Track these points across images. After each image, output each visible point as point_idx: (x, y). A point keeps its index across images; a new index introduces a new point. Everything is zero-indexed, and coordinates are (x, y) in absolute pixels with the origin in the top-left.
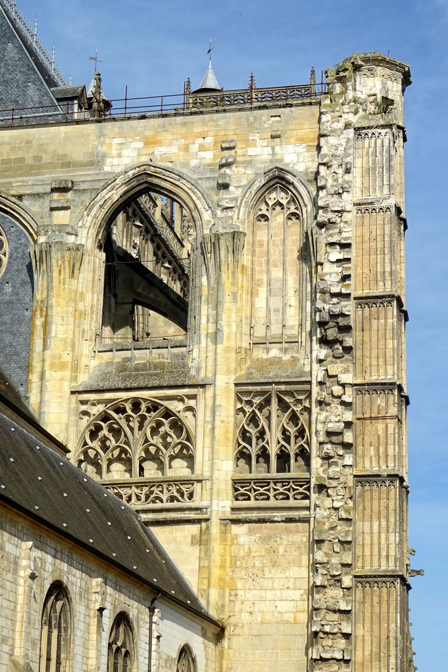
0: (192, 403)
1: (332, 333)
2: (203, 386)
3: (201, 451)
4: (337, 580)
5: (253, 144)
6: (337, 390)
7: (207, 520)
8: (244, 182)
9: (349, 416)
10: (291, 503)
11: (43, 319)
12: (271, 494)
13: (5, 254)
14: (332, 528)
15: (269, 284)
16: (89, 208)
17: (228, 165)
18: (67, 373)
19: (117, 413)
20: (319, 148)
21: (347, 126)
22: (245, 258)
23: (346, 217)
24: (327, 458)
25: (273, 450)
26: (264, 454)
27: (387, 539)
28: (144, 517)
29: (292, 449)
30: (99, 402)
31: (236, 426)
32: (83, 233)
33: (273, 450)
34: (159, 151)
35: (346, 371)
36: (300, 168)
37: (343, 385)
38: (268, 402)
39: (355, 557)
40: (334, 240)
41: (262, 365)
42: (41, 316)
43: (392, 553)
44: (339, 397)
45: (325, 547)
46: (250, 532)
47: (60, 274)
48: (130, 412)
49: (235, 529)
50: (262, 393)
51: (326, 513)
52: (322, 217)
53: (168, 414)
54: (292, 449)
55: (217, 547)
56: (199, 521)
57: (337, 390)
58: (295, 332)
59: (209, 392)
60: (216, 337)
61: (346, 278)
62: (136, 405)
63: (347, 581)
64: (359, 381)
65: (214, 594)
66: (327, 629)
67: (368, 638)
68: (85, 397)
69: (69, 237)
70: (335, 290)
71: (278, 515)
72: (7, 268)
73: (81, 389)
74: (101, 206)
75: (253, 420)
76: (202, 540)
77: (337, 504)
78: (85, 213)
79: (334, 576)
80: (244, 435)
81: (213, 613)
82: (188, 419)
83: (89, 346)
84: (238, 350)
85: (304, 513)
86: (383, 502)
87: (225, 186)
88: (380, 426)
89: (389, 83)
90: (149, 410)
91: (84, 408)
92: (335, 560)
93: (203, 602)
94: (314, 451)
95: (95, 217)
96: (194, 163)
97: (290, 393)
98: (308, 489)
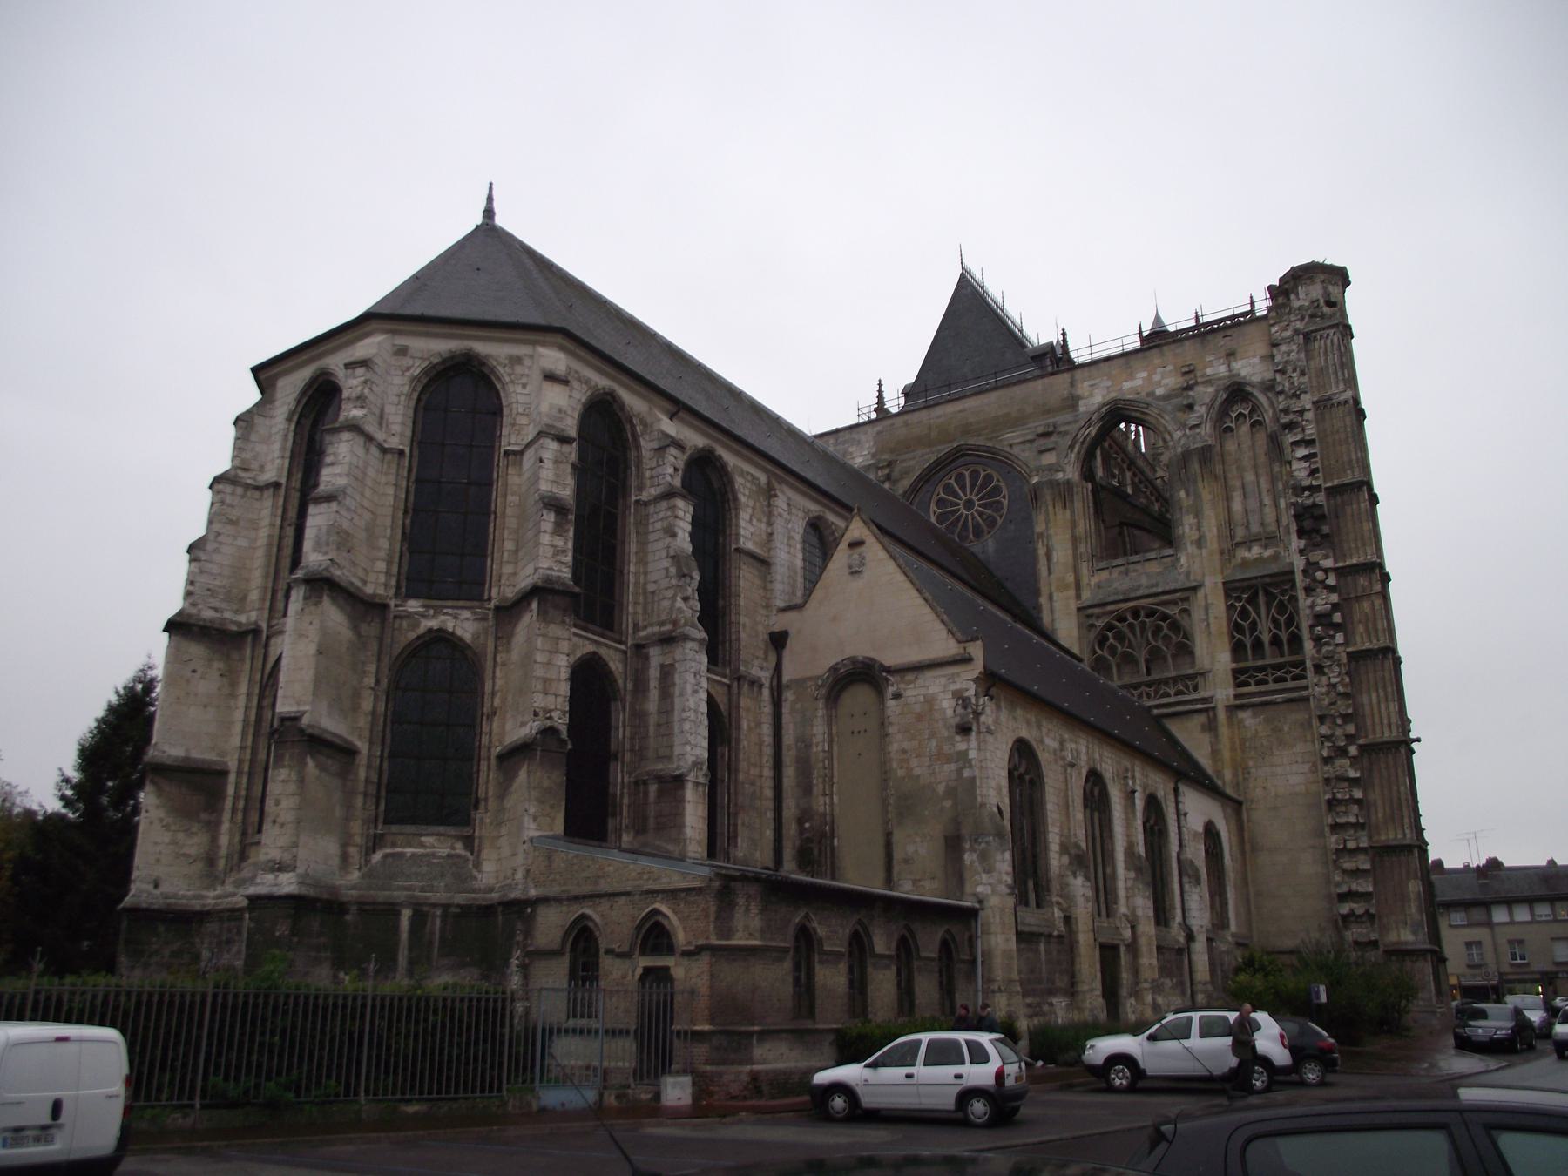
0: (1186, 606)
1: (1307, 524)
2: (1195, 589)
3: (1201, 647)
4: (1343, 752)
5: (1210, 364)
6: (1319, 575)
7: (1214, 708)
8: (1207, 400)
9: (1334, 598)
10: (1290, 684)
12: (1270, 679)
14: (1334, 703)
15: (1243, 487)
16: (1072, 447)
17: (1189, 388)
18: (1072, 592)
20: (1272, 357)
21: (1297, 332)
22: (1219, 469)
23: (1309, 415)
24: (1317, 640)
25: (1266, 638)
26: (1258, 644)
27: (1387, 708)
28: (1156, 711)
29: (1284, 636)
31: (1229, 619)
32: (1069, 469)
33: (1266, 638)
34: (1127, 385)
35: (1326, 557)
36: (1256, 379)
37: (1326, 571)
38: (1256, 594)
39: (1357, 728)
40: (1298, 438)
41: (1245, 564)
43: (1393, 720)
44: (1322, 582)
45: (1328, 721)
46: (1255, 715)
48: (1130, 620)
49: (1242, 715)
50: (1249, 587)
51: (1324, 690)
52: (1285, 419)
53: (1165, 617)
54: (1284, 636)
55: (1224, 731)
56: (1206, 710)
57: (1319, 575)
58: (1273, 527)
59: (1200, 594)
60: (1200, 543)
61: (1313, 472)
62: (1135, 613)
63: (1353, 750)
64: (1340, 565)
65: (1228, 774)
66: (1339, 796)
67: (1379, 803)
68: (1090, 611)
70: (1306, 483)
71: (1279, 697)
75: (1244, 614)
76: (1211, 727)
77: (1334, 680)
79: (1339, 748)
80: (1237, 628)
81: (1229, 791)
82: (1184, 622)
84: (1222, 553)
85: (1304, 693)
86: (1380, 674)
87: (1190, 407)
88: (1366, 605)
89: (1331, 288)
90: (1148, 616)
92: (1339, 732)
93: (1219, 783)
94: (1305, 634)
96: (1159, 391)
97: (1276, 585)
98: (1304, 670)
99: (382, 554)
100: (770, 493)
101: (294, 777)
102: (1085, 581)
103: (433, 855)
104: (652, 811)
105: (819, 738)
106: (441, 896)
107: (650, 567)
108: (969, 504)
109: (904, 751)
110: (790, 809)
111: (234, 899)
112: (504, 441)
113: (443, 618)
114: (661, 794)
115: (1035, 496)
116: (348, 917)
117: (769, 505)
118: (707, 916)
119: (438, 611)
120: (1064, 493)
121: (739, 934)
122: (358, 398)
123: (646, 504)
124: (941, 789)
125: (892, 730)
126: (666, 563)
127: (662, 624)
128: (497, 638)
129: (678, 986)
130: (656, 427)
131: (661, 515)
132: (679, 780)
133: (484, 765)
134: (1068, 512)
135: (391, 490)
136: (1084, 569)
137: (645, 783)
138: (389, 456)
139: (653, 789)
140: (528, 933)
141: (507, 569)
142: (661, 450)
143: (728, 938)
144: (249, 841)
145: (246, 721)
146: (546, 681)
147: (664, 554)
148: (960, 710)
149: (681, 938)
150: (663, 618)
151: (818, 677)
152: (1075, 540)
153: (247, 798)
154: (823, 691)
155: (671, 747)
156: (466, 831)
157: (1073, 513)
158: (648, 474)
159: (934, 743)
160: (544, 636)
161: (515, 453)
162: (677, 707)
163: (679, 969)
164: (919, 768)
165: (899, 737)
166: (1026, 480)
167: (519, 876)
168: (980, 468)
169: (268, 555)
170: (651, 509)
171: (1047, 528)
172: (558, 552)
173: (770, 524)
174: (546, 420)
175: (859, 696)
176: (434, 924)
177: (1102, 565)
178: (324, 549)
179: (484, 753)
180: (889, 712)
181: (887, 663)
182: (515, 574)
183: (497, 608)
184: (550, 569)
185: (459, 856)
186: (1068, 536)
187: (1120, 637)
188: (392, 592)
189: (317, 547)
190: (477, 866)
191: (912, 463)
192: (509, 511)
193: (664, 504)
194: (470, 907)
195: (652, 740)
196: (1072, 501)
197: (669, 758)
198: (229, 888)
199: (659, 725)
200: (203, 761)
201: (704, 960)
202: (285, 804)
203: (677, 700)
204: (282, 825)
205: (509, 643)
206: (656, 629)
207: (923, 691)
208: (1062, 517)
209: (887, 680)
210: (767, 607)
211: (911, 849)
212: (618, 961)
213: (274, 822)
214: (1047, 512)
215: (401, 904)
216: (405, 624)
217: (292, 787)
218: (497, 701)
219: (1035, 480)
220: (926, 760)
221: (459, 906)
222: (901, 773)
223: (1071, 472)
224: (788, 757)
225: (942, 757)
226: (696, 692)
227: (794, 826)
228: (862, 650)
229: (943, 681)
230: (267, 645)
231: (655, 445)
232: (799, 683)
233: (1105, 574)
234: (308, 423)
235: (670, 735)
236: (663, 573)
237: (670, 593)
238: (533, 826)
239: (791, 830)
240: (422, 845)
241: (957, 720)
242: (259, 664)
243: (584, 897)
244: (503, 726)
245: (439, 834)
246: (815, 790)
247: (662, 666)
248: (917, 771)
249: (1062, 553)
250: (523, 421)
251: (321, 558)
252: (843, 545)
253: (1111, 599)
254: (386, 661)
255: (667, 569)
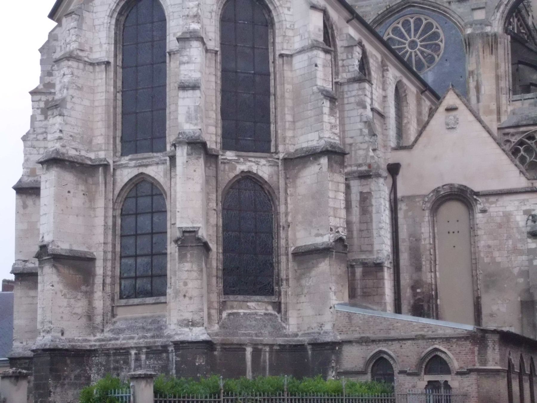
11: (475, 83)
13: (441, 41)
16: (498, 7)
18: (495, 117)
19: (529, 140)
30: (517, 133)
42: (473, 81)
47: (484, 53)
68: (507, 131)
69: (487, 27)
72: (444, 50)
73: (504, 126)
74: (506, 5)
78: (496, 11)
83: (506, 97)
91: (506, 138)
95: (503, 13)
99: (212, 121)
100: (383, 68)
101: (195, 267)
102: (503, 108)
103: (256, 314)
104: (359, 285)
105: (426, 235)
106: (267, 339)
107: (347, 128)
108: (413, 44)
109: (489, 247)
110: (406, 280)
111: (118, 342)
112: (278, 47)
113: (249, 164)
114: (365, 274)
115: (468, 43)
116: (216, 353)
117: (383, 76)
118: (473, 353)
119: (246, 159)
120: (491, 42)
121: (490, 363)
122: (195, 16)
123: (341, 84)
124: (516, 271)
125: (479, 232)
126: (360, 126)
127: (360, 165)
128: (286, 178)
129: (454, 392)
130: (345, 31)
131: (354, 93)
132: (379, 266)
133: (283, 259)
134: (493, 57)
135: (213, 79)
136: (504, 99)
137: (352, 266)
138: (209, 55)
139: (359, 271)
140: (338, 362)
141: (289, 134)
142: (349, 48)
143: (485, 366)
144: (116, 303)
145: (106, 226)
146: (335, 209)
147: (358, 119)
148: (530, 223)
149: (455, 365)
150: (360, 161)
151: (425, 196)
152: (498, 78)
153: (113, 277)
154: (429, 205)
155: (372, 245)
156: (274, 299)
157: (497, 57)
158: (340, 63)
159: (510, 242)
160: (332, 181)
161: (287, 56)
162: (374, 220)
163: (455, 382)
164: (499, 257)
165: (485, 237)
166: (461, 29)
167: (328, 327)
168: (422, 17)
169: (107, 112)
170: (346, 88)
171: (477, 68)
172: (333, 126)
173: (384, 89)
174: (313, 37)
175: (454, 210)
176: (265, 355)
177: (517, 97)
178: (195, 122)
179: (282, 251)
180: (478, 221)
181: (476, 189)
182: (294, 137)
183: (285, 160)
184: (330, 138)
185: (271, 314)
186: (493, 75)
187: (529, 150)
188: (219, 146)
189: (189, 119)
190: (286, 320)
191: (368, 9)
192: (287, 95)
193: (356, 86)
194: (284, 345)
195: (355, 239)
196: (497, 49)
197: (371, 252)
198: (107, 335)
199: (361, 231)
200: (81, 252)
201: (473, 376)
202: (190, 285)
203: (374, 216)
204: (191, 298)
205: (294, 182)
206: (355, 168)
207: (501, 209)
208: (489, 60)
209: (476, 200)
210: (385, 146)
211: (495, 308)
212: (409, 378)
213: (185, 296)
214: (478, 56)
215: (246, 345)
216: (227, 167)
217: (195, 274)
218: (290, 219)
219: (469, 31)
220: (505, 253)
221: (280, 345)
222: (486, 260)
223: (496, 26)
224: (403, 247)
225: (516, 251)
226: (385, 210)
227: (409, 290)
228: (458, 180)
229: (517, 203)
230: (114, 175)
231: (345, 44)
232: (410, 198)
233: (518, 104)
234: (123, 19)
235: (370, 237)
236: (359, 132)
237: (365, 146)
238: (334, 298)
239: (407, 293)
240: (248, 308)
241: (529, 229)
242: (110, 187)
243: (380, 341)
244: (295, 235)
245: (258, 301)
246: (424, 268)
247: (361, 193)
248: (498, 259)
249: (488, 88)
250: (290, 33)
251: (193, 127)
252: (441, 109)
253: (524, 123)
254: (220, 192)
255: (361, 130)
